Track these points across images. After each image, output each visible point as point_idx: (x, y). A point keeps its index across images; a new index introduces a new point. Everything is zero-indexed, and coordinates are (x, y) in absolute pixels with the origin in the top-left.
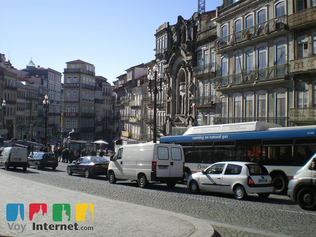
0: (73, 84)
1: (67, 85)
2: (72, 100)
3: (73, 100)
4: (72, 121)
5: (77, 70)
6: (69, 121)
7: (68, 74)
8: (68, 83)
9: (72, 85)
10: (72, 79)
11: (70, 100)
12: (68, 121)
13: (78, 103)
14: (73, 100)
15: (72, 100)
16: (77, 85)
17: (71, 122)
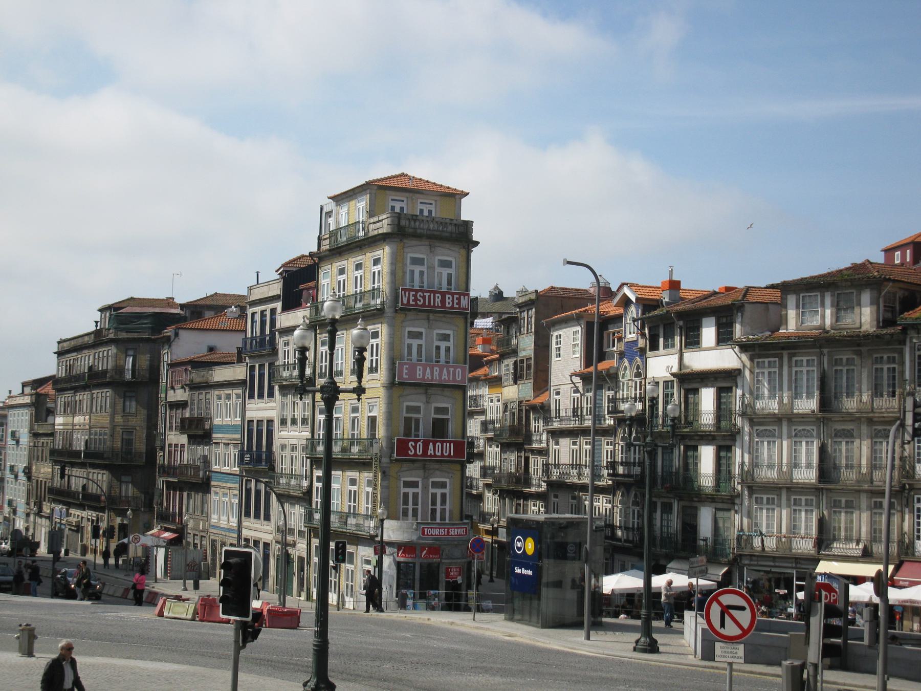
0: (443, 294)
1: (416, 300)
2: (436, 373)
3: (440, 374)
4: (431, 480)
5: (450, 228)
6: (414, 485)
7: (414, 242)
8: (417, 291)
9: (438, 300)
10: (431, 268)
11: (428, 376)
12: (408, 484)
13: (458, 394)
14: (440, 374)
15: (436, 373)
16: (459, 303)
17: (425, 488)
